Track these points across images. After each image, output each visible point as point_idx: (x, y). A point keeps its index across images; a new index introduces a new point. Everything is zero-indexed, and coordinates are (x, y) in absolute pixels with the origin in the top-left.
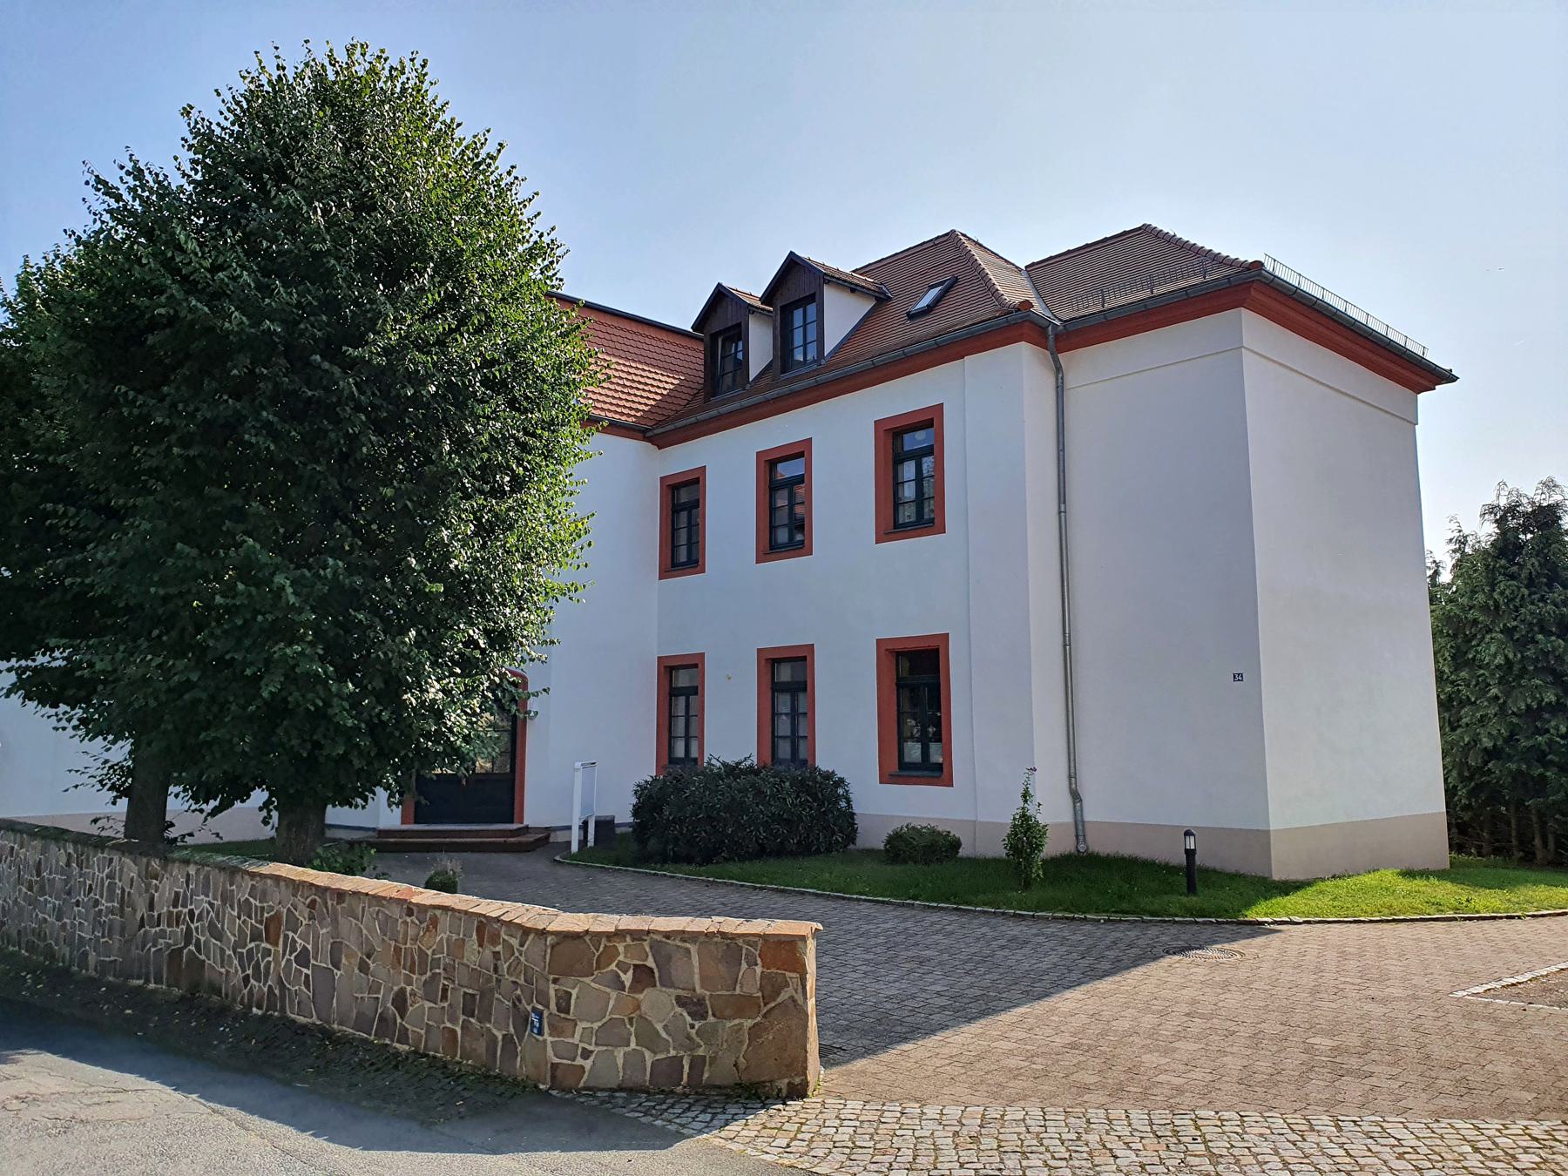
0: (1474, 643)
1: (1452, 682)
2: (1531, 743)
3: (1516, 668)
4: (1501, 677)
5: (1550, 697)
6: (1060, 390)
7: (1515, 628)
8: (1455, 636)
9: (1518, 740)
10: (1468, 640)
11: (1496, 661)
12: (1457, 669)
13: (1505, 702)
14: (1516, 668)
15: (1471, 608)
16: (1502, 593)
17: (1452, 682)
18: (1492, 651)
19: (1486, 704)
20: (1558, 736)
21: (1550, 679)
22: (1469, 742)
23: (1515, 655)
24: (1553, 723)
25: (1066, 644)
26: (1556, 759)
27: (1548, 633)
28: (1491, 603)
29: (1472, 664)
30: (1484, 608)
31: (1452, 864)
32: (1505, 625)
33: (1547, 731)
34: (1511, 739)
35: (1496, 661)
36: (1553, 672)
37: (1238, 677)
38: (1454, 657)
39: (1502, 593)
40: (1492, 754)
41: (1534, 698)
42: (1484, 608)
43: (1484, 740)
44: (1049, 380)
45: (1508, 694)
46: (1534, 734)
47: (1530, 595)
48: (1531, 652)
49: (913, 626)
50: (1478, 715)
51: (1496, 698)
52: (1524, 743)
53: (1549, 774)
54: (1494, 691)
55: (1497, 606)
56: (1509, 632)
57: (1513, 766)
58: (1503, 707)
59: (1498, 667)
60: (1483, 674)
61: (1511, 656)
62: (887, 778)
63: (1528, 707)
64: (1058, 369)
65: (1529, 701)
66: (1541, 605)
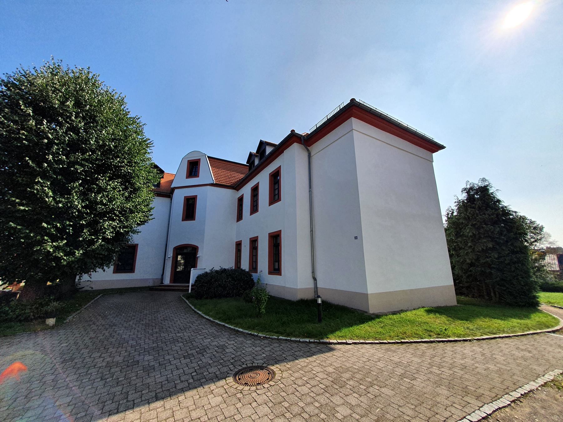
0: (462, 230)
1: (456, 242)
2: (484, 261)
3: (477, 237)
4: (472, 240)
5: (490, 245)
6: (310, 156)
7: (476, 224)
8: (456, 228)
9: (480, 260)
10: (461, 229)
11: (470, 235)
12: (457, 238)
13: (474, 248)
14: (477, 237)
15: (460, 219)
16: (470, 213)
17: (456, 242)
18: (468, 231)
19: (467, 248)
20: (494, 258)
21: (490, 239)
22: (463, 261)
23: (476, 232)
24: (492, 254)
25: (312, 231)
26: (495, 266)
27: (487, 224)
28: (466, 216)
29: (461, 236)
30: (465, 218)
31: (458, 301)
32: (472, 223)
33: (490, 257)
34: (478, 259)
35: (470, 235)
36: (490, 237)
37: (356, 238)
38: (456, 235)
39: (470, 213)
40: (472, 265)
41: (484, 246)
42: (465, 218)
43: (467, 260)
44: (306, 154)
45: (475, 245)
46: (486, 258)
47: (479, 213)
48: (482, 231)
49: (274, 230)
50: (465, 252)
51: (471, 247)
52: (482, 261)
53: (492, 272)
54: (469, 244)
55: (469, 218)
56: (473, 225)
57: (479, 269)
58: (474, 250)
59: (471, 236)
60: (466, 239)
61: (474, 233)
62: (270, 273)
63: (483, 249)
64: (308, 150)
65: (482, 247)
66: (483, 215)
